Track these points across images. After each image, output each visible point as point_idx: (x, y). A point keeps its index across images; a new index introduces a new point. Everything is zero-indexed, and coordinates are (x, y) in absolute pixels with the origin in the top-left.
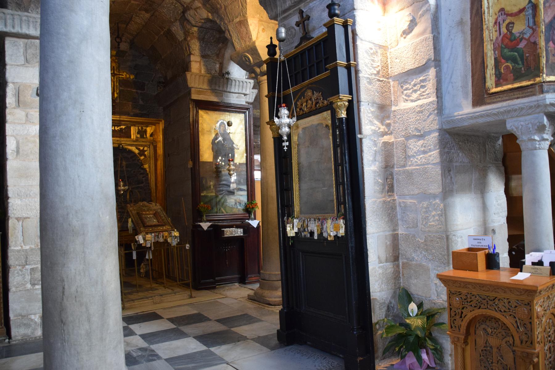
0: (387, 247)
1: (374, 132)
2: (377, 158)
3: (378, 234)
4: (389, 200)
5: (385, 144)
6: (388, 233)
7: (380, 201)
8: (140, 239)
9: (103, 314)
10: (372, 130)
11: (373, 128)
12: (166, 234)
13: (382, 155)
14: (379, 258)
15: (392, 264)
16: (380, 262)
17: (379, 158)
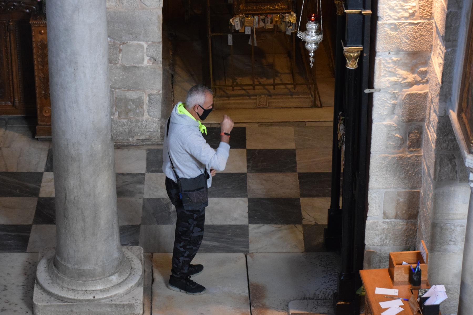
0: (398, 203)
1: (395, 83)
2: (396, 111)
3: (385, 190)
4: (409, 156)
5: (411, 96)
6: (402, 190)
7: (394, 158)
8: (236, 22)
9: (95, 217)
10: (390, 82)
11: (393, 79)
12: (277, 18)
13: (404, 108)
14: (384, 213)
15: (405, 221)
16: (385, 216)
17: (399, 111)
